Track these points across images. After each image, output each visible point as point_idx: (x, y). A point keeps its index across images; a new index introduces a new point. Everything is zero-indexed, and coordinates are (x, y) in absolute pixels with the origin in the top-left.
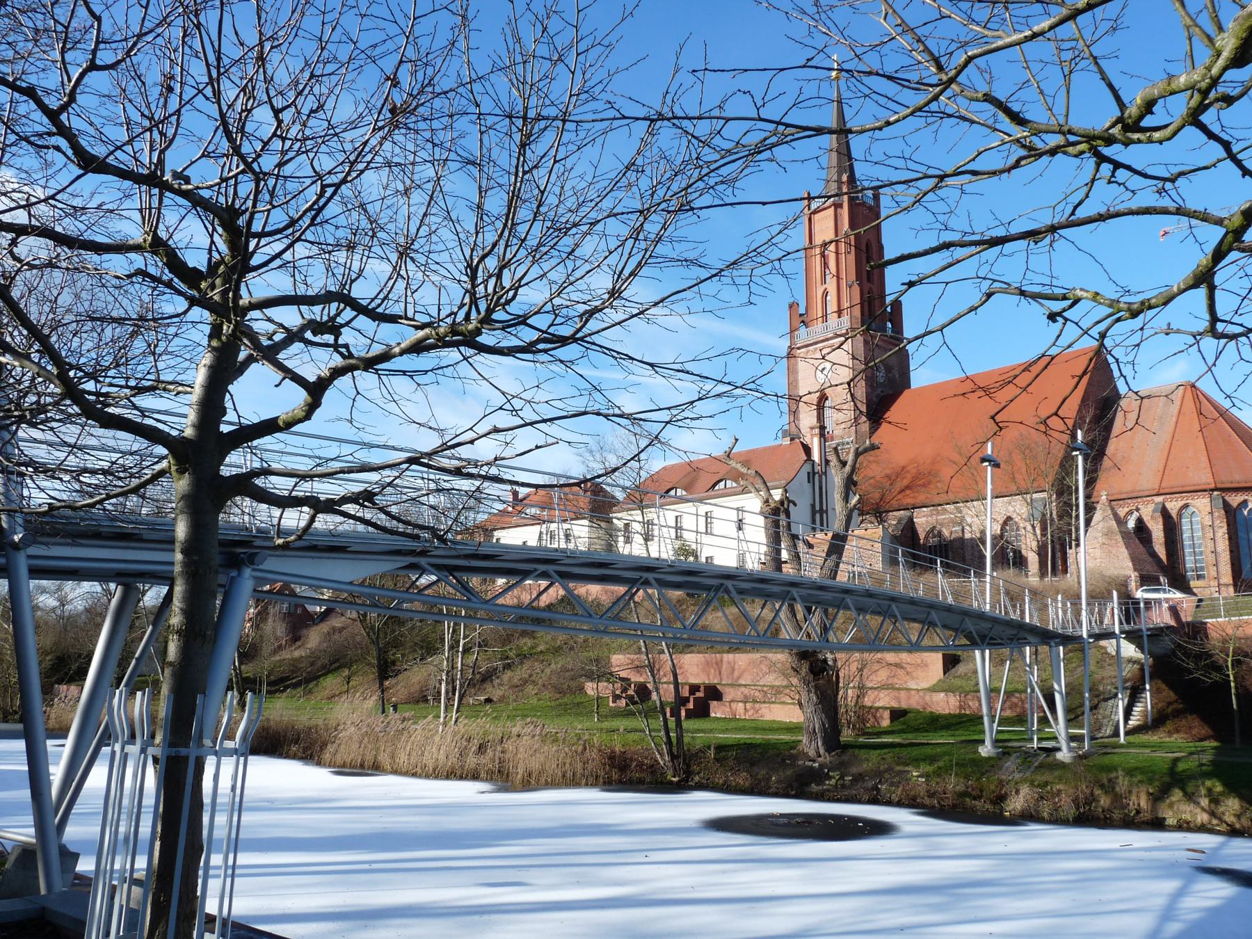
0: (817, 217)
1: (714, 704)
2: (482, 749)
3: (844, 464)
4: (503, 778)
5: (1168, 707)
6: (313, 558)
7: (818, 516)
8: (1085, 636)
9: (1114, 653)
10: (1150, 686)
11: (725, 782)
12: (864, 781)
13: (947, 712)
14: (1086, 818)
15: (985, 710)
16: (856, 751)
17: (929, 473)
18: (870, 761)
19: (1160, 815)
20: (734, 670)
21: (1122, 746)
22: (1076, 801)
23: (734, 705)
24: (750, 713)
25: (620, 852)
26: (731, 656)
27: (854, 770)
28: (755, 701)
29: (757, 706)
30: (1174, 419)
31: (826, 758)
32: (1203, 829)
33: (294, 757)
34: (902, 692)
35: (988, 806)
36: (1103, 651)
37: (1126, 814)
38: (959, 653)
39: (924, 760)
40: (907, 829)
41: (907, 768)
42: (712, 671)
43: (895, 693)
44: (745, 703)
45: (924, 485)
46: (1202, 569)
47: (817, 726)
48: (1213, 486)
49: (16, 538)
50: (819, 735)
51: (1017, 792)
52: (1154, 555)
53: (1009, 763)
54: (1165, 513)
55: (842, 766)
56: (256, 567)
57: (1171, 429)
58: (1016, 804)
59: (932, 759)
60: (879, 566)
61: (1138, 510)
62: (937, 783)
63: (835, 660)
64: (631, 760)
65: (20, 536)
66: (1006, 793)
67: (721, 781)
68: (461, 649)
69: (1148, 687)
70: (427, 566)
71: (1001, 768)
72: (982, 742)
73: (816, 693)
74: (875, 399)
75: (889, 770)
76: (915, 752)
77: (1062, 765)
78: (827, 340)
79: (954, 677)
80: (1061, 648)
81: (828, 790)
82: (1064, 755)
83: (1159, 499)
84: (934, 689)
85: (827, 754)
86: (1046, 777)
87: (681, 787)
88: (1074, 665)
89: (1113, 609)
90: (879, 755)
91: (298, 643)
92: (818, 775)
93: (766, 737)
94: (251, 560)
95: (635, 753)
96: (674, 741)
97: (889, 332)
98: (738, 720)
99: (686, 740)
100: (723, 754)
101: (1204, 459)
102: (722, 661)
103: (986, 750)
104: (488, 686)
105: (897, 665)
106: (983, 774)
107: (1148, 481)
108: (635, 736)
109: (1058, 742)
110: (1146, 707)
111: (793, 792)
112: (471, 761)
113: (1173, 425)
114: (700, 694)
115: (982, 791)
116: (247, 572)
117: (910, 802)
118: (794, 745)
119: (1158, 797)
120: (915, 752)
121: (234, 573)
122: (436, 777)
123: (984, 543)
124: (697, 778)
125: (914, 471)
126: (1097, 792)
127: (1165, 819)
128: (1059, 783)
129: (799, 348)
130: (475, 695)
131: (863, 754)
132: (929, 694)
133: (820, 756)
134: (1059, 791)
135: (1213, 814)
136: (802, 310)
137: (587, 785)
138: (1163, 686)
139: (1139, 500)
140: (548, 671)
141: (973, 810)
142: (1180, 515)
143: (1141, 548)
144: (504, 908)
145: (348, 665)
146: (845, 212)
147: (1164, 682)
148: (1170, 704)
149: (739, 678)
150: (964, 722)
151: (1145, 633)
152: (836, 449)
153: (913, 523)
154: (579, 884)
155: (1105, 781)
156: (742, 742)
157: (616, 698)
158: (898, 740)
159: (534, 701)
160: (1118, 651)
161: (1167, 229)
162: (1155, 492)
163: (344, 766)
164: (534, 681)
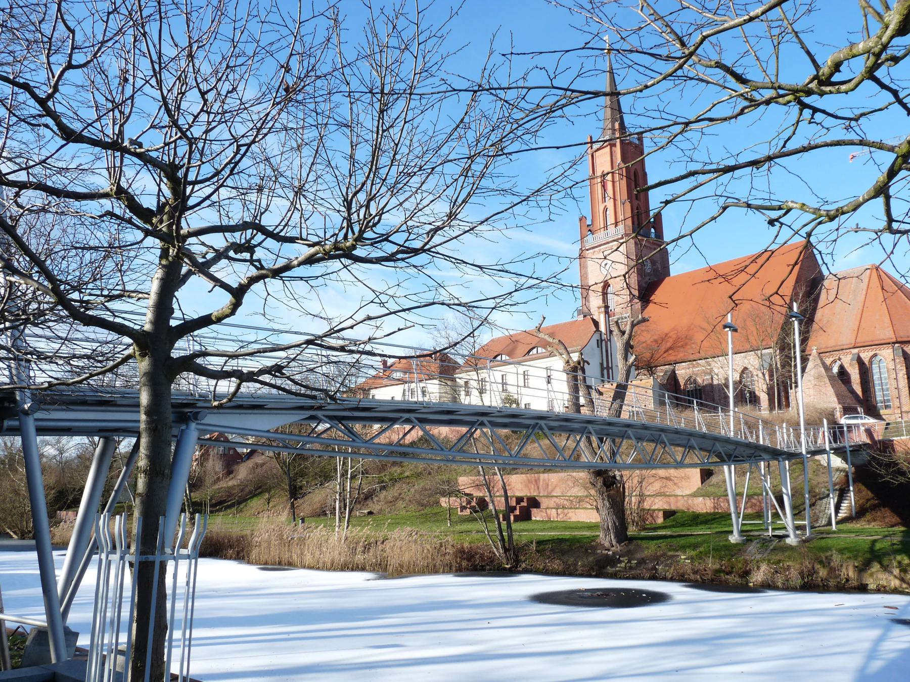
0: (597, 153)
1: (534, 511)
3: (623, 333)
4: (383, 569)
5: (867, 503)
6: (240, 414)
7: (605, 371)
8: (804, 452)
9: (826, 465)
11: (544, 567)
12: (646, 563)
13: (705, 511)
14: (809, 586)
15: (732, 509)
16: (639, 542)
18: (649, 549)
19: (864, 582)
20: (548, 485)
21: (834, 532)
22: (801, 574)
23: (549, 511)
24: (561, 516)
25: (469, 620)
26: (546, 475)
27: (638, 556)
28: (564, 508)
29: (566, 511)
30: (864, 292)
31: (617, 548)
32: (895, 591)
33: (230, 558)
34: (671, 498)
35: (737, 579)
36: (817, 463)
37: (838, 582)
38: (712, 468)
39: (689, 547)
40: (678, 597)
41: (677, 553)
43: (667, 499)
44: (557, 509)
45: (682, 346)
46: (889, 401)
47: (610, 525)
48: (894, 340)
49: (26, 407)
50: (612, 531)
51: (758, 568)
52: (853, 392)
53: (751, 548)
54: (860, 361)
55: (629, 554)
57: (863, 300)
58: (758, 577)
59: (695, 546)
60: (651, 406)
61: (840, 359)
62: (699, 563)
63: (621, 476)
64: (476, 554)
65: (29, 405)
67: (541, 567)
68: (349, 476)
69: (851, 488)
70: (323, 418)
71: (745, 552)
72: (732, 532)
73: (608, 501)
74: (644, 285)
75: (664, 555)
76: (682, 541)
77: (790, 548)
78: (608, 243)
79: (710, 486)
80: (787, 462)
81: (620, 571)
82: (792, 541)
83: (856, 351)
84: (694, 495)
85: (618, 545)
86: (780, 556)
88: (797, 474)
89: (824, 432)
90: (656, 544)
91: (231, 476)
92: (612, 561)
94: (195, 417)
95: (478, 547)
96: (506, 538)
97: (653, 236)
98: (553, 521)
99: (515, 537)
100: (542, 547)
101: (887, 320)
102: (539, 479)
103: (734, 538)
104: (369, 502)
105: (667, 478)
106: (732, 556)
107: (847, 338)
108: (479, 535)
109: (787, 531)
110: (851, 503)
111: (594, 573)
112: (359, 558)
114: (524, 504)
115: (732, 568)
116: (193, 426)
117: (680, 578)
118: (594, 538)
119: (862, 569)
120: (682, 541)
121: (183, 427)
122: (335, 570)
123: (727, 387)
124: (524, 565)
125: (674, 336)
126: (817, 566)
127: (867, 584)
129: (587, 250)
130: (360, 509)
131: (644, 544)
133: (613, 546)
134: (789, 567)
135: (902, 580)
136: (589, 222)
137: (444, 572)
138: (863, 488)
139: (841, 352)
140: (413, 490)
141: (726, 581)
142: (871, 362)
143: (843, 387)
144: (386, 663)
145: (268, 490)
147: (863, 484)
148: (868, 500)
149: (552, 491)
151: (848, 449)
152: (617, 322)
153: (675, 374)
154: (440, 644)
156: (556, 537)
157: (463, 508)
159: (403, 512)
161: (854, 154)
162: (852, 346)
163: (266, 563)
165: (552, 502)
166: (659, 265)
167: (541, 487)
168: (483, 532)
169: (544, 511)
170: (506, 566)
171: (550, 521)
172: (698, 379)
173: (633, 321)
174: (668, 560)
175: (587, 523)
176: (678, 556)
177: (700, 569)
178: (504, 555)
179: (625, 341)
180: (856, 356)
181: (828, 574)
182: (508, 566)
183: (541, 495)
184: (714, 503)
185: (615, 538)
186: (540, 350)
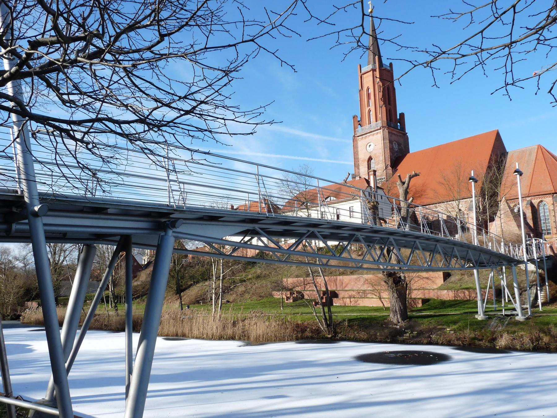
0: (364, 76)
1: (335, 300)
2: (234, 324)
3: (404, 183)
6: (202, 224)
9: (524, 269)
10: (548, 283)
12: (423, 334)
13: (448, 299)
14: (537, 349)
15: (479, 297)
16: (416, 319)
17: (422, 191)
18: (425, 325)
20: (343, 283)
21: (541, 312)
22: (531, 340)
23: (345, 300)
24: (353, 303)
26: (341, 277)
28: (354, 297)
29: (356, 299)
30: (534, 162)
31: (402, 324)
35: (487, 344)
38: (450, 271)
39: (451, 323)
40: (456, 357)
41: (443, 327)
42: (332, 284)
44: (350, 298)
45: (419, 197)
46: (549, 230)
47: (397, 309)
48: (554, 192)
49: (36, 208)
50: (398, 313)
51: (502, 336)
53: (492, 323)
54: (532, 205)
56: (175, 230)
57: (533, 167)
58: (502, 342)
59: (455, 323)
63: (405, 277)
65: (39, 207)
66: (495, 337)
67: (352, 337)
68: (221, 278)
69: (547, 284)
71: (490, 325)
72: (477, 312)
73: (396, 293)
74: (394, 158)
77: (518, 323)
78: (371, 132)
81: (406, 339)
82: (520, 318)
83: (530, 198)
84: (440, 289)
85: (402, 322)
87: (333, 340)
90: (428, 321)
91: (136, 279)
92: (400, 332)
93: (369, 314)
94: (173, 224)
95: (308, 324)
96: (328, 317)
97: (399, 128)
98: (347, 306)
99: (334, 317)
100: (351, 323)
101: (549, 179)
102: (337, 279)
103: (480, 317)
105: (427, 278)
106: (482, 328)
110: (547, 294)
111: (389, 340)
112: (230, 332)
113: (533, 165)
115: (483, 337)
116: (170, 232)
117: (449, 344)
120: (445, 319)
121: (163, 234)
122: (215, 340)
124: (340, 335)
125: (414, 190)
126: (541, 335)
128: (521, 332)
129: (358, 136)
131: (420, 321)
132: (440, 291)
133: (399, 323)
136: (359, 119)
137: (288, 340)
140: (254, 287)
141: (480, 346)
142: (538, 205)
144: (284, 411)
146: (377, 74)
147: (553, 281)
149: (345, 287)
150: (458, 303)
151: (545, 259)
152: (399, 176)
153: (415, 214)
155: (546, 330)
156: (358, 317)
157: (288, 298)
158: (432, 313)
159: (249, 301)
160: (526, 268)
161: (536, 72)
163: (167, 335)
164: (248, 292)
165: (346, 294)
166: (403, 146)
167: (338, 284)
168: (312, 313)
169: (342, 299)
170: (328, 336)
171: (345, 306)
172: (429, 216)
173: (410, 175)
174: (438, 331)
175: (371, 307)
176: (444, 329)
177: (461, 338)
178: (326, 329)
179: (405, 189)
180: (530, 202)
181: (550, 340)
182: (330, 336)
183: (338, 289)
184: (454, 294)
185: (400, 317)
186: (332, 198)
